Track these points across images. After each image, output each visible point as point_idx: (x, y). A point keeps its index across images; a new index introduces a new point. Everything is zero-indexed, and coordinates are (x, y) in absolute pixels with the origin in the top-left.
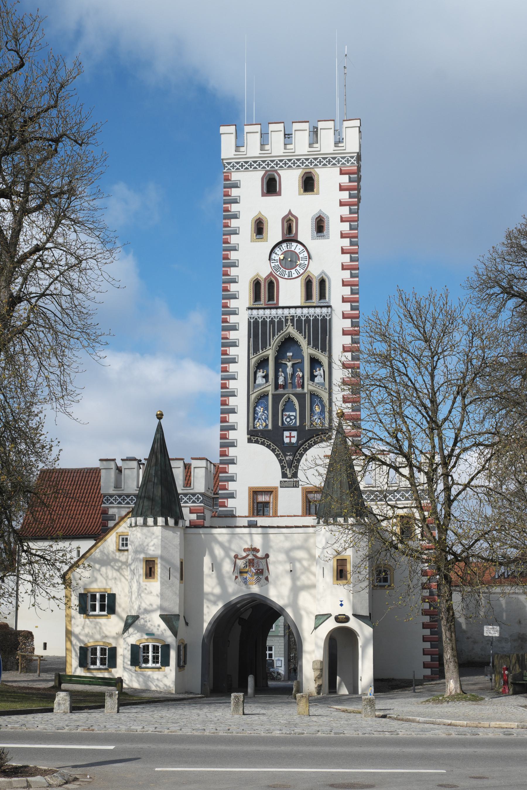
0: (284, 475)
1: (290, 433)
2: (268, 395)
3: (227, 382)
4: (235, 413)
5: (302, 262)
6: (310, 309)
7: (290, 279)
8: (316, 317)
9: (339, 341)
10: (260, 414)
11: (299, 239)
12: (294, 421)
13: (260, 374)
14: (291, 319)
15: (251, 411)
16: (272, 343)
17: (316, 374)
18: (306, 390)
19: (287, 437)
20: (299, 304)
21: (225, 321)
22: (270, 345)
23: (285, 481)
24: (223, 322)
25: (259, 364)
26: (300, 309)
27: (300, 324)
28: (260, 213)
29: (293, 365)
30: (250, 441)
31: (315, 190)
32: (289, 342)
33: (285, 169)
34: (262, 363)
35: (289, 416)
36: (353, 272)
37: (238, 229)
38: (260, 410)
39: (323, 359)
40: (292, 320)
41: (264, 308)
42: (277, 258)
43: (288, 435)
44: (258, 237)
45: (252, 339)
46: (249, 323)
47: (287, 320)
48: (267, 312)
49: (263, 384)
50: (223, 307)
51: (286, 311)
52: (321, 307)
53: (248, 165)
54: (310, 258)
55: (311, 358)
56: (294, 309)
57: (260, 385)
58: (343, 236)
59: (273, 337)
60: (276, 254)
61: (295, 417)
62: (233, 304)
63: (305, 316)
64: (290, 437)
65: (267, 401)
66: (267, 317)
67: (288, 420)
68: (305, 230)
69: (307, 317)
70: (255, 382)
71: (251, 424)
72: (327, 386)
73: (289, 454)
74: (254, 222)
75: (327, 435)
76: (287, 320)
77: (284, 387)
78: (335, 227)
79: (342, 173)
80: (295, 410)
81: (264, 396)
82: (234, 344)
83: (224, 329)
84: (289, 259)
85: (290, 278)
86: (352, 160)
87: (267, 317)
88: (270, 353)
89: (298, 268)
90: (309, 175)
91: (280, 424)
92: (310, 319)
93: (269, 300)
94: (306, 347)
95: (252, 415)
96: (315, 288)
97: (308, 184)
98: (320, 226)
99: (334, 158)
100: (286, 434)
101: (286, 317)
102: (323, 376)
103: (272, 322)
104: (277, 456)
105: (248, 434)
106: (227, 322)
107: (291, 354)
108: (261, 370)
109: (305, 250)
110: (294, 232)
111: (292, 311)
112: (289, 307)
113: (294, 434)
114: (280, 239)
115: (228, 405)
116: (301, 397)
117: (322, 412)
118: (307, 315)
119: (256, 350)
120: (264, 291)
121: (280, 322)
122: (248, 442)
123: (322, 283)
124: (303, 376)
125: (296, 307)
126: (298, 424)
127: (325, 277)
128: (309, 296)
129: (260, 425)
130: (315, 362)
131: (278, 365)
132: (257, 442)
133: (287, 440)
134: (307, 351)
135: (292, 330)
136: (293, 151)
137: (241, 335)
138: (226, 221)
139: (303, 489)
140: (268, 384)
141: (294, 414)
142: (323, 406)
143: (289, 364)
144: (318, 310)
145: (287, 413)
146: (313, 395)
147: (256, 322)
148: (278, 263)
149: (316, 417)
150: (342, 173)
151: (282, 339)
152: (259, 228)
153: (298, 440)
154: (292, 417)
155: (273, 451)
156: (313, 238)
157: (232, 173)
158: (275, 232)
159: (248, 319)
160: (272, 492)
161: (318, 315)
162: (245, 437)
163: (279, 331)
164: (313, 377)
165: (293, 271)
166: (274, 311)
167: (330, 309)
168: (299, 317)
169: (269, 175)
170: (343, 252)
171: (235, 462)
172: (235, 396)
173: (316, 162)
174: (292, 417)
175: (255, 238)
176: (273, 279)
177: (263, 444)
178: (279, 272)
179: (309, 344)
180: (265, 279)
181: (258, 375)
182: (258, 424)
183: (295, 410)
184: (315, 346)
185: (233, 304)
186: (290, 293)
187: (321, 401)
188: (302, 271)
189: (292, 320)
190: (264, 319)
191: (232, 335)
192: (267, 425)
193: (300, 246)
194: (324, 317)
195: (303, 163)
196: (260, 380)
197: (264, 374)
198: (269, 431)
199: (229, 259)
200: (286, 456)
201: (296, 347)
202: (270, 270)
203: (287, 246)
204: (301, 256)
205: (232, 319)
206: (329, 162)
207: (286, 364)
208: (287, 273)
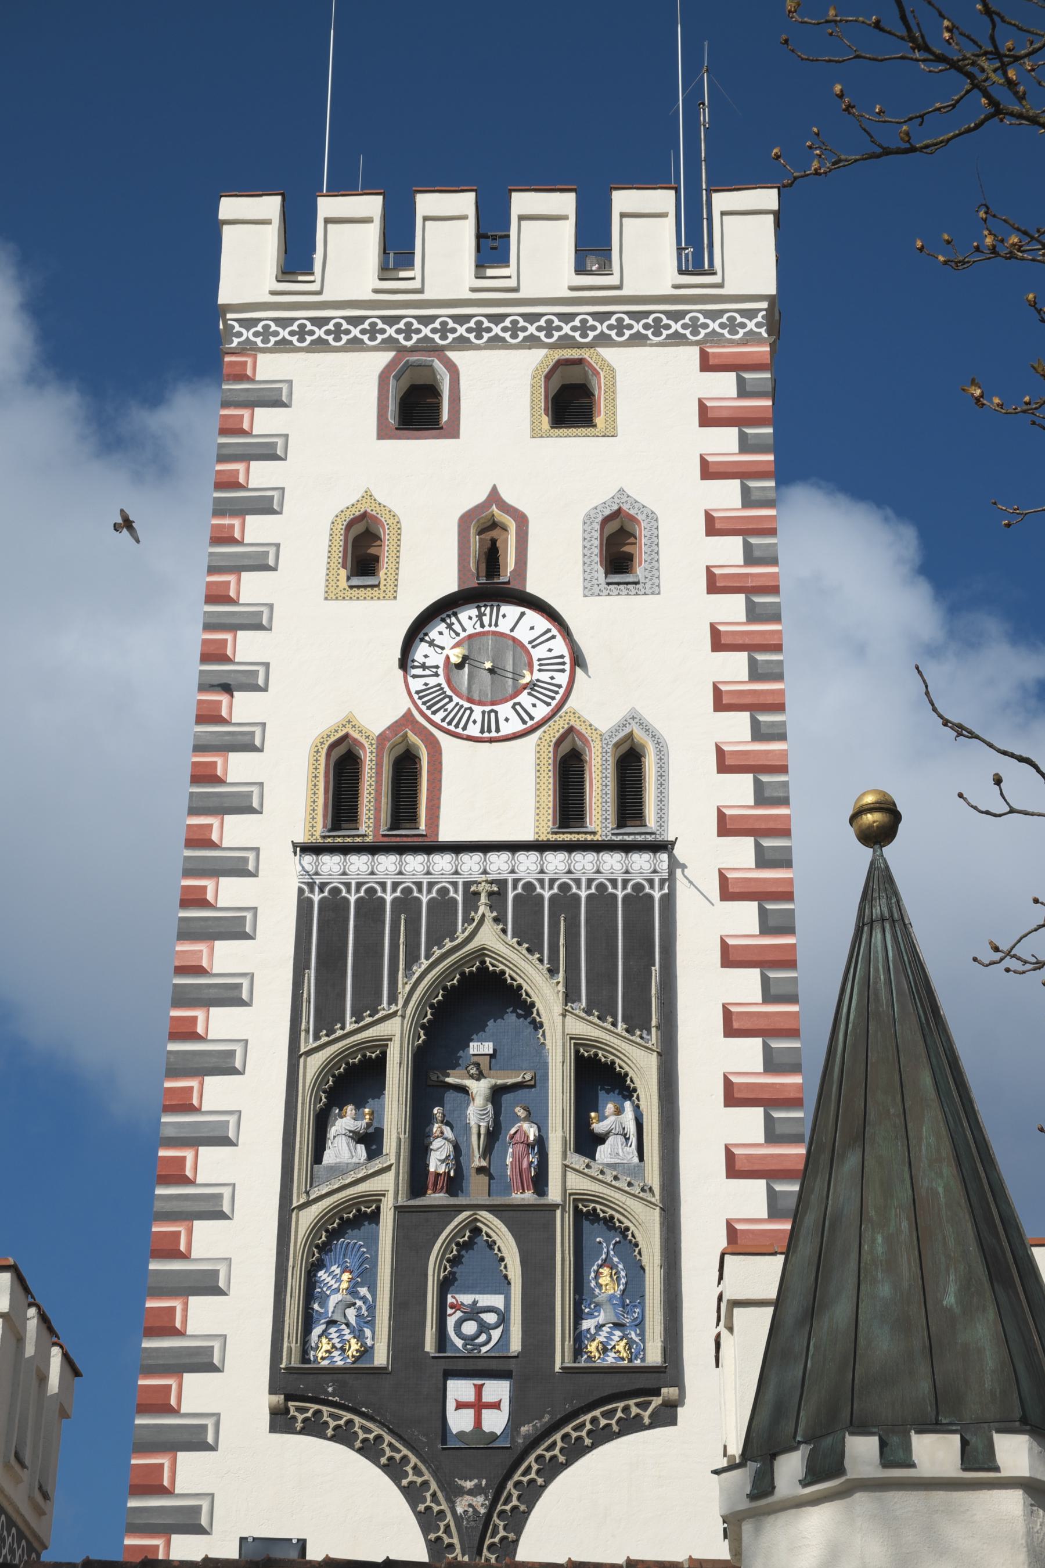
1: (479, 1389)
2: (375, 1217)
3: (188, 1154)
4: (219, 1292)
5: (545, 676)
6: (578, 856)
7: (491, 740)
8: (601, 887)
9: (705, 988)
10: (333, 1300)
11: (532, 587)
12: (496, 1334)
13: (345, 1123)
14: (490, 894)
15: (295, 1281)
16: (403, 990)
17: (599, 1127)
18: (554, 1195)
19: (460, 1405)
20: (529, 836)
21: (195, 899)
22: (393, 999)
24: (185, 904)
25: (339, 1080)
26: (534, 856)
27: (528, 914)
28: (368, 495)
29: (497, 1094)
30: (281, 1421)
31: (599, 420)
32: (479, 997)
33: (478, 348)
34: (356, 1080)
35: (473, 1313)
36: (762, 718)
37: (272, 551)
38: (335, 1280)
39: (641, 1064)
40: (497, 897)
41: (373, 850)
42: (436, 659)
43: (469, 1396)
44: (356, 581)
46: (304, 906)
47: (472, 898)
48: (387, 863)
49: (357, 1166)
50: (190, 843)
51: (471, 864)
52: (627, 848)
53: (329, 332)
54: (578, 660)
55: (579, 1059)
56: (505, 856)
57: (338, 1170)
58: (715, 584)
59: (408, 967)
60: (431, 643)
61: (504, 1319)
62: (234, 832)
63: (552, 881)
64: (477, 1409)
65: (373, 1241)
66: (383, 885)
67: (470, 1328)
68: (556, 562)
69: (564, 887)
70: (318, 1158)
71: (291, 1344)
72: (653, 1176)
73: (469, 1485)
74: (340, 528)
75: (656, 1402)
76: (472, 898)
77: (454, 1184)
78: (682, 551)
79: (707, 365)
80: (503, 1285)
81: (355, 1219)
82: (231, 996)
83: (189, 932)
84: (488, 665)
85: (490, 736)
86: (751, 325)
87: (383, 885)
88: (396, 1033)
89: (524, 698)
90: (573, 376)
91: (429, 1345)
92: (577, 898)
93: (395, 824)
94: (557, 1007)
95: (300, 1300)
96: (602, 786)
97: (571, 402)
98: (618, 549)
99: (676, 316)
100: (459, 1389)
101: (467, 885)
102: (633, 1139)
103: (407, 904)
104: (412, 1494)
105: (272, 1391)
106: (204, 904)
107: (488, 1048)
108: (350, 1109)
109: (554, 632)
110: (511, 565)
111: (499, 863)
112: (485, 848)
113: (498, 1390)
114: (450, 585)
115: (185, 1256)
116: (531, 1224)
117: (633, 1293)
118: (565, 879)
119: (328, 1017)
120: (375, 789)
121: (443, 906)
122: (274, 1428)
123: (629, 763)
124: (541, 1144)
125: (514, 847)
126: (516, 1345)
127: (640, 735)
128: (569, 805)
129: (329, 1350)
130: (597, 1078)
131: (428, 1093)
132: (314, 1428)
133: (459, 1422)
134: (560, 1024)
135: (494, 940)
136: (512, 283)
137: (266, 961)
138: (226, 521)
140: (377, 1164)
141: (497, 1301)
142: (637, 1270)
143: (480, 1088)
144: (612, 862)
145: (467, 1299)
146: (587, 1216)
147: (334, 906)
148: (441, 680)
149: (601, 1319)
150: (707, 365)
151: (448, 974)
152: (363, 552)
153: (514, 1421)
154: (492, 1313)
155: (394, 1470)
156: (588, 591)
157: (261, 357)
158: (428, 565)
159: (301, 891)
161: (614, 882)
162: (261, 1401)
163: (435, 940)
164: (587, 1141)
165: (505, 710)
166: (415, 863)
167: (664, 857)
168: (529, 886)
169: (408, 366)
170: (719, 642)
171: (204, 1521)
172: (221, 1216)
173: (602, 328)
174: (492, 1313)
175: (343, 583)
176: (414, 738)
177: (343, 1436)
178: (441, 714)
179: (570, 996)
180: (382, 738)
181: (332, 1131)
182: (325, 1345)
183: (503, 1285)
184: (601, 1007)
185: (234, 832)
186: (490, 790)
188: (541, 712)
189: (497, 897)
190: (371, 891)
191: (225, 958)
192: (366, 1352)
193: (533, 617)
194: (638, 887)
195: (549, 329)
196: (340, 1149)
197: (360, 1125)
198: (380, 1371)
199: (226, 659)
200: (453, 1492)
201: (511, 1018)
202: (404, 705)
203: (480, 616)
204: (537, 653)
205: (229, 893)
206: (657, 328)
207: (463, 1090)
208: (477, 715)
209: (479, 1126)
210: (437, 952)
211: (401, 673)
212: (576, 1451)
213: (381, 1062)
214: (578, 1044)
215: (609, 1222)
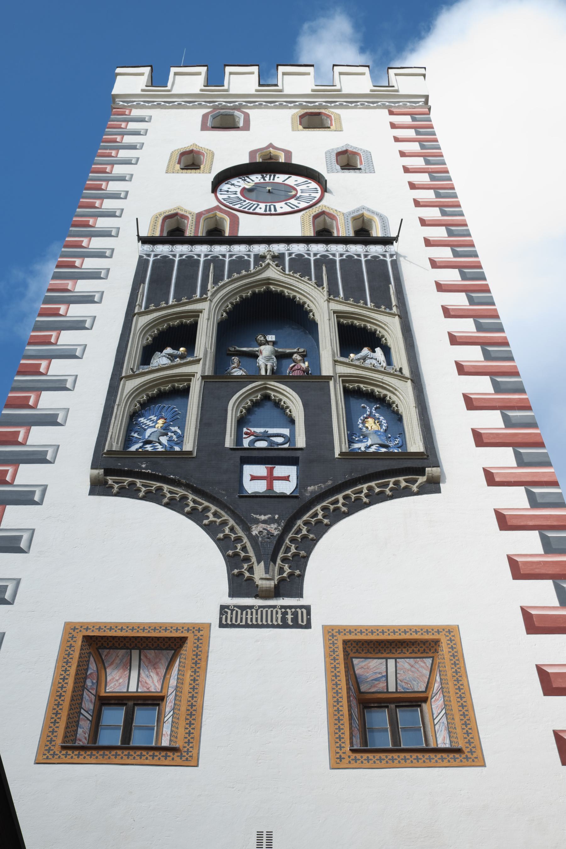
0: (240, 584)
1: (271, 471)
2: (186, 392)
23: (243, 608)
25: (162, 334)
45: (145, 288)
65: (185, 407)
73: (263, 517)
75: (422, 479)
105: (93, 467)
122: (92, 492)
132: (129, 492)
139: (330, 632)
149: (369, 442)
153: (301, 484)
160: (182, 641)
179: (333, 292)
187: (384, 404)
209: (266, 365)
210: (236, 275)
211: (213, 195)
212: (356, 506)
213: (194, 327)
214: (339, 315)
215: (371, 397)
